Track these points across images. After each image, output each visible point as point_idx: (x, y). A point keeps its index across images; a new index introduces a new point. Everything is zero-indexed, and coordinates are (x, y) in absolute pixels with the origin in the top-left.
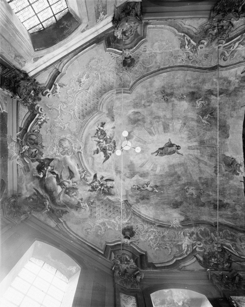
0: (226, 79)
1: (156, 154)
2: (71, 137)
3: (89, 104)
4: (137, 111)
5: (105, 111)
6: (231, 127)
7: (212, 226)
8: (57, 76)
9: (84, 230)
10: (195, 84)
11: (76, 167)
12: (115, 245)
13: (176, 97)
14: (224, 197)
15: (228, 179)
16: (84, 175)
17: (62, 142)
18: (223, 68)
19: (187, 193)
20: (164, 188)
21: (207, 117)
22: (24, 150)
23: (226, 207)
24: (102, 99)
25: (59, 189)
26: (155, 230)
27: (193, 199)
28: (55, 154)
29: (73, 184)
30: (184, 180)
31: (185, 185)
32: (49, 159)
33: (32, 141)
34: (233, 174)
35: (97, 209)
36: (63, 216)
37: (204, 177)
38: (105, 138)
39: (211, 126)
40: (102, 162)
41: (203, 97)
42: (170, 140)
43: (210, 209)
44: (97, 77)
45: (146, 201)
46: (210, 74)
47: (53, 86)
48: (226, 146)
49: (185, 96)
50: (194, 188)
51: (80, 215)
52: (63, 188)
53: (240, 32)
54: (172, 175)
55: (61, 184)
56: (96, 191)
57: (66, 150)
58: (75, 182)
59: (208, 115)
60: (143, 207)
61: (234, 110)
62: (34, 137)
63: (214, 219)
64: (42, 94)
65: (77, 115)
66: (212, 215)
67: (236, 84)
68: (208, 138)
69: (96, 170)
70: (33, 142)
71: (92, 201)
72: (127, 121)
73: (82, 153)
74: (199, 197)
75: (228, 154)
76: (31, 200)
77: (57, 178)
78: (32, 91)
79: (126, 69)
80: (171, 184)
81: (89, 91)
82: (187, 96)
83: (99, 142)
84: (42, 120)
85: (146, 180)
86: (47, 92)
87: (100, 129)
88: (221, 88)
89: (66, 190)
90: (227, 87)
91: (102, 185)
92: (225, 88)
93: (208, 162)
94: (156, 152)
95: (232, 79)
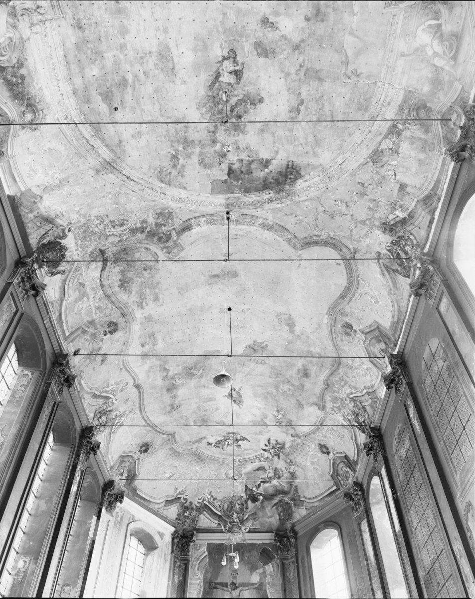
0: (148, 372)
3: (190, 460)
7: (327, 388)
8: (169, 501)
9: (315, 486)
11: (255, 464)
12: (333, 468)
22: (237, 519)
24: (183, 452)
31: (277, 391)
32: (246, 490)
33: (229, 509)
35: (297, 460)
39: (205, 366)
42: (223, 396)
47: (178, 496)
49: (172, 395)
57: (236, 473)
62: (226, 506)
65: (202, 466)
70: (230, 507)
71: (289, 461)
73: (239, 458)
74: (293, 385)
77: (264, 482)
78: (186, 514)
80: (277, 401)
83: (228, 444)
84: (209, 497)
85: (270, 415)
86: (184, 499)
91: (274, 448)
92: (158, 369)
95: (146, 367)
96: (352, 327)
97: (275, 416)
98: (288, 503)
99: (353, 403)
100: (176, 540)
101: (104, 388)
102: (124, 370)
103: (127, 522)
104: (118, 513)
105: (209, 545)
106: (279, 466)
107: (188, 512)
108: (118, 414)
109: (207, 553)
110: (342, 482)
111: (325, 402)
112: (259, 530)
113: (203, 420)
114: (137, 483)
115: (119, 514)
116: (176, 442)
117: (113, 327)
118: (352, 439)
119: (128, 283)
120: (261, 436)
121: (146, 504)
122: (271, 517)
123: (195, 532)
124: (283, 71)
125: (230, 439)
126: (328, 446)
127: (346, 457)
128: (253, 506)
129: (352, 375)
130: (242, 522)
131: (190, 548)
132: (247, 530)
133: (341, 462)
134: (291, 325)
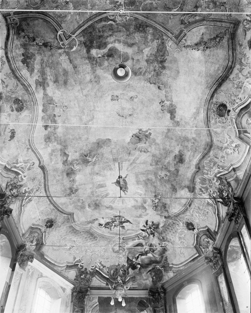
0: (51, 155)
1: (125, 192)
2: (112, 244)
4: (88, 206)
5: (90, 225)
6: (99, 138)
7: (198, 171)
8: (70, 266)
9: (181, 255)
10: (59, 176)
12: (197, 240)
13: (73, 185)
14: (172, 151)
15: (154, 144)
16: (141, 237)
17: (115, 250)
18: (41, 161)
19: (164, 178)
20: (158, 192)
21: (90, 158)
22: (121, 281)
23: (183, 153)
25: (150, 255)
26: (192, 210)
27: (170, 176)
28: (124, 256)
29: (147, 245)
30: (151, 177)
31: (156, 177)
32: (128, 260)
33: (115, 274)
34: (150, 138)
35: (168, 237)
36: (169, 262)
37: (150, 162)
38: (111, 222)
39: (98, 154)
40: (132, 224)
41: (71, 166)
42: (113, 183)
43: (182, 167)
44: (65, 239)
45: (167, 206)
46: (48, 168)
47: (76, 264)
48: (119, 141)
49: (71, 179)
50: (160, 171)
51: (170, 251)
52: (149, 252)
53: (9, 173)
54: (146, 184)
55: (146, 253)
56: (154, 233)
58: (146, 244)
59: (87, 158)
60: (172, 210)
61: (80, 138)
62: (112, 272)
63: (192, 167)
64: (82, 268)
65: (94, 242)
66: (189, 167)
67: (54, 145)
68: (111, 155)
69: (137, 229)
70: (115, 273)
71: (162, 238)
72: (97, 210)
73: (123, 236)
74: (169, 171)
75: (128, 139)
76: (154, 277)
77: (142, 255)
78: (82, 277)
79: (55, 223)
81: (75, 240)
82: (71, 178)
83: (115, 226)
86: (81, 266)
87: (104, 227)
88: (60, 156)
89: (151, 251)
90: (58, 151)
91: (150, 228)
92: (59, 153)
93: (135, 156)
94: (124, 192)
95: (49, 150)
96: (226, 107)
97: (153, 201)
98: (159, 270)
99: (219, 182)
100: (75, 294)
101: (14, 163)
102: (30, 150)
103: (37, 277)
104: (29, 269)
105: (99, 298)
106: (154, 243)
107: (83, 275)
108: (27, 190)
109: (98, 303)
110: (203, 250)
111: (195, 184)
112: (137, 288)
113: (95, 204)
114: (45, 250)
115: (30, 270)
116: (74, 222)
118: (215, 213)
119: (31, 59)
120: (141, 219)
121: (52, 266)
122: (146, 279)
123: (89, 289)
125: (116, 221)
126: (194, 223)
127: (208, 230)
128: (133, 272)
129: (221, 155)
130: (124, 283)
131: (85, 300)
132: (128, 288)
133: (204, 235)
134: (172, 112)
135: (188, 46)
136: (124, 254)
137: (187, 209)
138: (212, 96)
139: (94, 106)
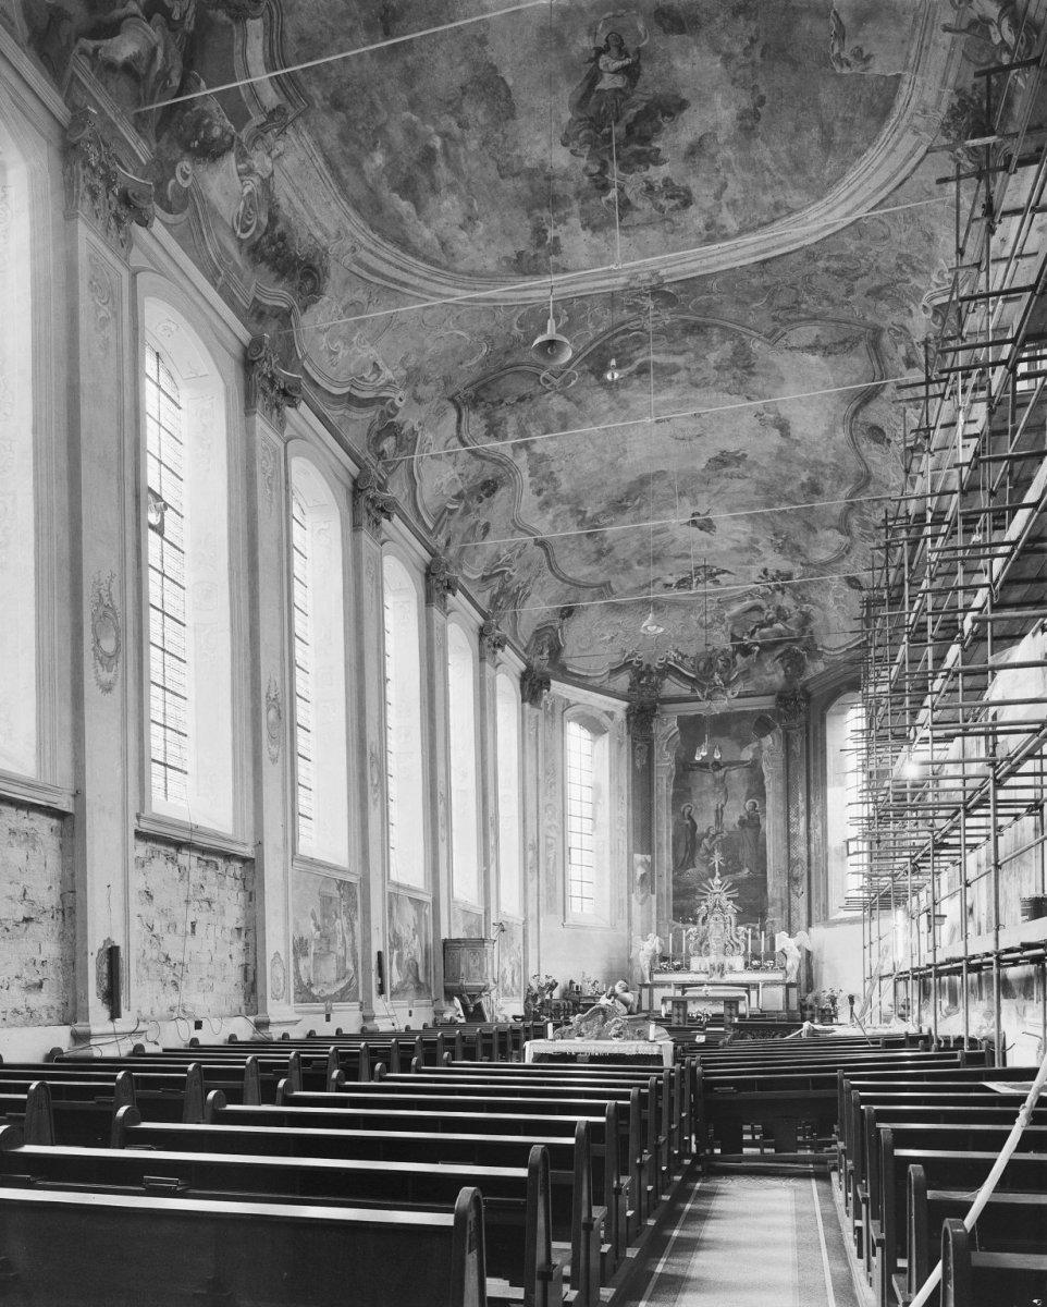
44: (599, 625)
55: (771, 623)
59: (624, 503)
62: (702, 664)
77: (762, 625)
83: (698, 582)
86: (637, 662)
95: (550, 517)
98: (799, 654)
117: (489, 487)
122: (773, 673)
124: (719, 52)
130: (728, 684)
132: (736, 695)
135: (792, 349)
136: (724, 628)
137: (843, 557)
138: (856, 413)
139: (623, 437)
